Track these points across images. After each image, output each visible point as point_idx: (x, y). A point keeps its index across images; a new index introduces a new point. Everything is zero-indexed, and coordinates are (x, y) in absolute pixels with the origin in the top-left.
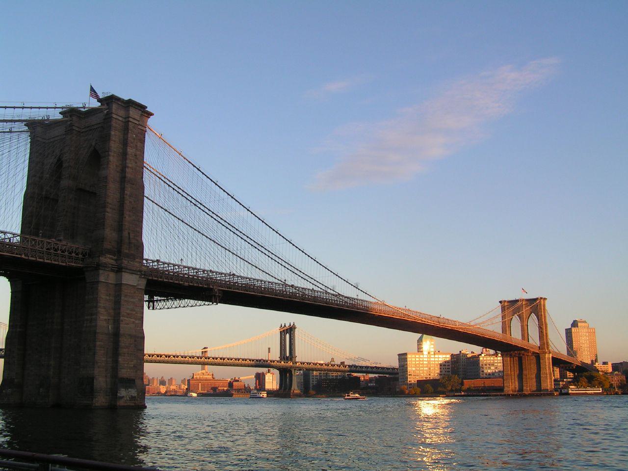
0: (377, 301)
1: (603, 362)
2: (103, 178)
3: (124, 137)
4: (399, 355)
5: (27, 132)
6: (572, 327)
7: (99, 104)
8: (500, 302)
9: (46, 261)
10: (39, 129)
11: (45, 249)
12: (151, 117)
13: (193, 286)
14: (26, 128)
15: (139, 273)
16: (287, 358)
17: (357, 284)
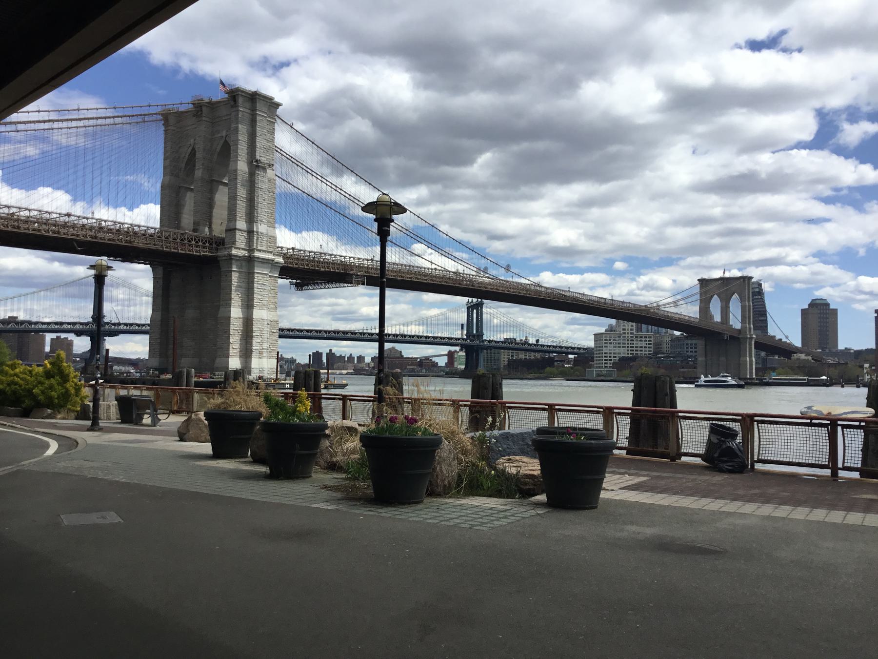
0: (532, 283)
1: (282, 366)
2: (234, 170)
3: (252, 130)
4: (595, 335)
5: (162, 120)
6: (809, 307)
7: (227, 96)
8: (699, 280)
9: (180, 251)
10: (172, 120)
11: (178, 240)
12: (280, 107)
13: (330, 271)
14: (160, 117)
15: (271, 262)
16: (474, 336)
17: (508, 266)
